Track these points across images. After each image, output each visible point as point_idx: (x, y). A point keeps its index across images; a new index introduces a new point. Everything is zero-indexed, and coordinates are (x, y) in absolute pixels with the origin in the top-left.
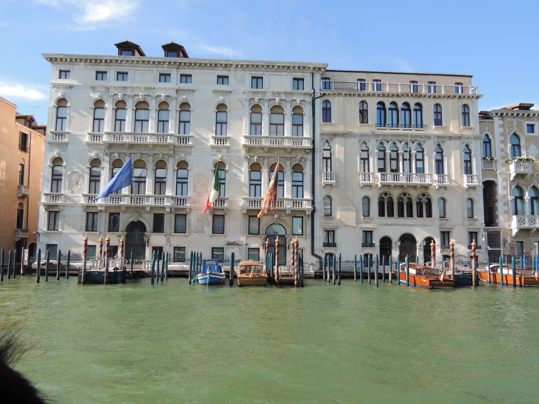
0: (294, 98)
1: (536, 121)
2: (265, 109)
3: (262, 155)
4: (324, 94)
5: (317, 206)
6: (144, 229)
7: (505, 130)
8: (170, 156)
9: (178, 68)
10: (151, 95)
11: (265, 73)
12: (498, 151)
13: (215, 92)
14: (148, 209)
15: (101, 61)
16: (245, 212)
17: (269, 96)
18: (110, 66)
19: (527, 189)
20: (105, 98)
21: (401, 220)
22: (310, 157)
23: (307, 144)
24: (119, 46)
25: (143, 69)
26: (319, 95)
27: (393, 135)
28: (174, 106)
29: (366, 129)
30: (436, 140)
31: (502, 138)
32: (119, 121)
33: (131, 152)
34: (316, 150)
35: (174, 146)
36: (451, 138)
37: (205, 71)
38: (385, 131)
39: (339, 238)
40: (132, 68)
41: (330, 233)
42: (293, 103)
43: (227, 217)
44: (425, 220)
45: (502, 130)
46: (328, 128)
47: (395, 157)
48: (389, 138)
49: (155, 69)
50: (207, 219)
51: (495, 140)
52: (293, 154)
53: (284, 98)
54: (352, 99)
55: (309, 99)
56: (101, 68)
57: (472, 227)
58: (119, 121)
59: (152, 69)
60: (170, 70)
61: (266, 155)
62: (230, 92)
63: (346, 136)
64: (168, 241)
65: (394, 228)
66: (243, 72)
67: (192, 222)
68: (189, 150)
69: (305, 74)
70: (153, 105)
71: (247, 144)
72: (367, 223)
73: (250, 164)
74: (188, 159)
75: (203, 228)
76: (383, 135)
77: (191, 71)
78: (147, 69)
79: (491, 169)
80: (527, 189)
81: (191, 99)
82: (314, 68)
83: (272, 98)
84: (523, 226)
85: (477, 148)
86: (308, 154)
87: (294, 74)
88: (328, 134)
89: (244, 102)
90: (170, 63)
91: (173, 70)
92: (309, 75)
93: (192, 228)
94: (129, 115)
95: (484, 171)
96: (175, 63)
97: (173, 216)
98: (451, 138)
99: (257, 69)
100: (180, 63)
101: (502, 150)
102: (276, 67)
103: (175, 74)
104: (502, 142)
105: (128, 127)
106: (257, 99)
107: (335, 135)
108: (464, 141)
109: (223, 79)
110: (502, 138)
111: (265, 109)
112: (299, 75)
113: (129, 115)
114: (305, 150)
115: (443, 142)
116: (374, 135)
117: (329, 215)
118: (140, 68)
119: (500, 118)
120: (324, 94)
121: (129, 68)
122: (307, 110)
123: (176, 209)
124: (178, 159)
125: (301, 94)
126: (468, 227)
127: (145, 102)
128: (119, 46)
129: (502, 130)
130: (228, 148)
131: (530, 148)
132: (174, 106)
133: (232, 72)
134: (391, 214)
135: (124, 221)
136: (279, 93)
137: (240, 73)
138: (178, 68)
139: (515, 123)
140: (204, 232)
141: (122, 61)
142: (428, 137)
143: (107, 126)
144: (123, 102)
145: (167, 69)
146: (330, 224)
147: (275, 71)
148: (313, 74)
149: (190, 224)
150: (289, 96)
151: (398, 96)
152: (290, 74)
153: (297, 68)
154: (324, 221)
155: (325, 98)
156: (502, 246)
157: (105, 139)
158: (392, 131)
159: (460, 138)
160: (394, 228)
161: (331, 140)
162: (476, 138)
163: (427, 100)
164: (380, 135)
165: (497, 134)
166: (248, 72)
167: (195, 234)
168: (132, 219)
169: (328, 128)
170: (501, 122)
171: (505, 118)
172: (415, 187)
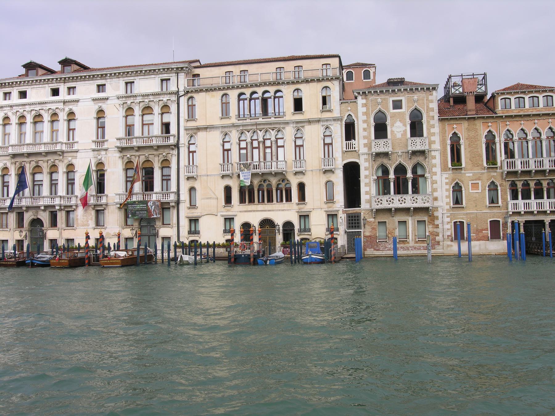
0: (161, 99)
1: (403, 96)
2: (137, 111)
3: (134, 154)
4: (188, 92)
5: (182, 198)
6: (42, 224)
7: (368, 109)
8: (60, 161)
9: (64, 83)
10: (44, 108)
11: (136, 78)
12: (361, 130)
13: (94, 100)
14: (43, 208)
15: (5, 83)
16: (119, 206)
17: (139, 99)
18: (13, 87)
19: (391, 167)
20: (10, 114)
21: (260, 207)
22: (175, 152)
23: (172, 141)
24: (24, 66)
25: (38, 86)
26: (183, 93)
27: (252, 125)
28: (62, 116)
29: (226, 122)
30: (294, 125)
31: (365, 118)
32: (21, 134)
33: (30, 160)
34: (180, 145)
35: (63, 152)
36: (310, 122)
37: (87, 82)
38: (245, 121)
39: (203, 225)
40: (30, 87)
41: (194, 221)
42: (161, 103)
43: (106, 211)
44: (285, 205)
45: (364, 110)
46: (192, 124)
47: (257, 146)
48: (249, 128)
49: (47, 85)
50: (91, 214)
51: (358, 120)
52: (161, 151)
53: (152, 100)
54: (214, 93)
55: (174, 98)
56: (7, 90)
57: (330, 209)
58: (21, 134)
59: (44, 86)
60: (59, 84)
61: (137, 154)
62: (107, 99)
63: (208, 130)
64: (61, 234)
65: (254, 214)
66: (118, 79)
67: (79, 217)
68: (74, 154)
69: (171, 75)
70: (47, 117)
71: (119, 145)
72: (228, 211)
73: (124, 163)
74: (74, 162)
75: (88, 221)
76: (243, 126)
77: (75, 83)
78: (41, 86)
79: (354, 149)
80: (391, 167)
81: (75, 108)
82: (177, 68)
83: (141, 100)
84: (380, 206)
85: (338, 131)
86: (173, 149)
87: (161, 76)
88: (192, 129)
89: (118, 106)
90: (57, 79)
91: (61, 84)
92: (174, 74)
93: (79, 222)
94: (29, 128)
95: (344, 153)
96: (61, 78)
97: (64, 213)
98: (310, 122)
99: (128, 75)
100: (65, 78)
101: (365, 130)
102: (144, 72)
103: (63, 89)
104: (364, 122)
105: (29, 139)
106: (129, 102)
107: (198, 129)
108: (324, 124)
109: (101, 88)
110: (365, 118)
111: (137, 111)
112: (165, 76)
113: (29, 128)
114: (168, 147)
115: (303, 127)
116: (234, 126)
117: (192, 206)
118: (35, 86)
119: (363, 97)
120: (188, 92)
121: (27, 87)
122: (173, 108)
123: (66, 207)
124: (66, 162)
125: (167, 94)
126: (327, 209)
127: (40, 115)
128: (24, 66)
129: (364, 110)
130: (106, 150)
131: (395, 125)
132: (62, 116)
133: (108, 80)
134: (251, 201)
135: (28, 217)
136: (148, 95)
137: (115, 80)
138: (64, 83)
139: (379, 100)
140: (89, 226)
141: (20, 82)
142: (287, 123)
143: (14, 139)
144: (23, 117)
145: (56, 84)
146: (195, 213)
147: (144, 75)
148: (178, 73)
149: (77, 219)
150: (157, 97)
151: (256, 86)
152: (158, 76)
153: (161, 70)
154: (189, 211)
155: (189, 95)
156: (362, 227)
157: (11, 151)
158: (252, 121)
159: (318, 121)
160: (254, 214)
161: (196, 133)
162: (335, 119)
163: (287, 87)
164: (240, 126)
165: (360, 114)
166: (121, 79)
167: (82, 227)
168: (33, 217)
169: (192, 124)
170: (364, 101)
171: (369, 96)
172: (270, 174)
